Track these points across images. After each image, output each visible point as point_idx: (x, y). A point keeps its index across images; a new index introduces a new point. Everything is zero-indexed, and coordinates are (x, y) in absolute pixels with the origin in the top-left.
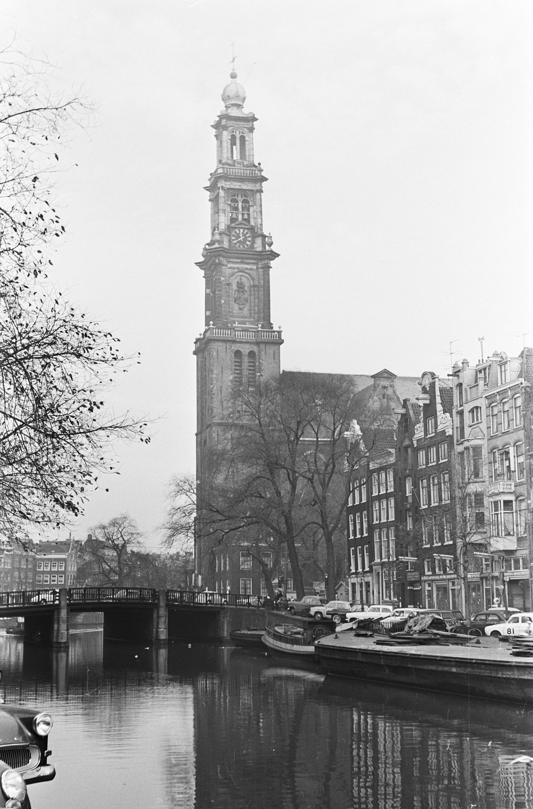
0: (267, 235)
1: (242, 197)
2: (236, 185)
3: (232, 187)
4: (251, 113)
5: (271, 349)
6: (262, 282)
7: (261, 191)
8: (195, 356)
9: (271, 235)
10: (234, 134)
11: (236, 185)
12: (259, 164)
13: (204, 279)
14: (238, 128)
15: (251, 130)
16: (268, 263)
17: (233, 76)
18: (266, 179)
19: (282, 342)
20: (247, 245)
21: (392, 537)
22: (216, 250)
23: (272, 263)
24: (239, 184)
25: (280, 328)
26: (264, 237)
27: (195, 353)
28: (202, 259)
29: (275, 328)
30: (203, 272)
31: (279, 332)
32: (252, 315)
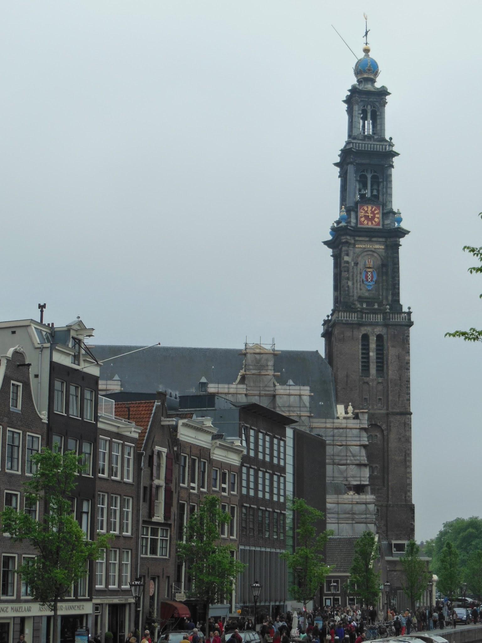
8: (323, 339)
9: (401, 211)
12: (391, 139)
13: (332, 258)
17: (367, 51)
18: (397, 154)
20: (375, 222)
21: (236, 464)
22: (345, 228)
23: (402, 241)
25: (409, 308)
26: (394, 213)
28: (330, 238)
29: (405, 309)
30: (330, 251)
31: (409, 313)
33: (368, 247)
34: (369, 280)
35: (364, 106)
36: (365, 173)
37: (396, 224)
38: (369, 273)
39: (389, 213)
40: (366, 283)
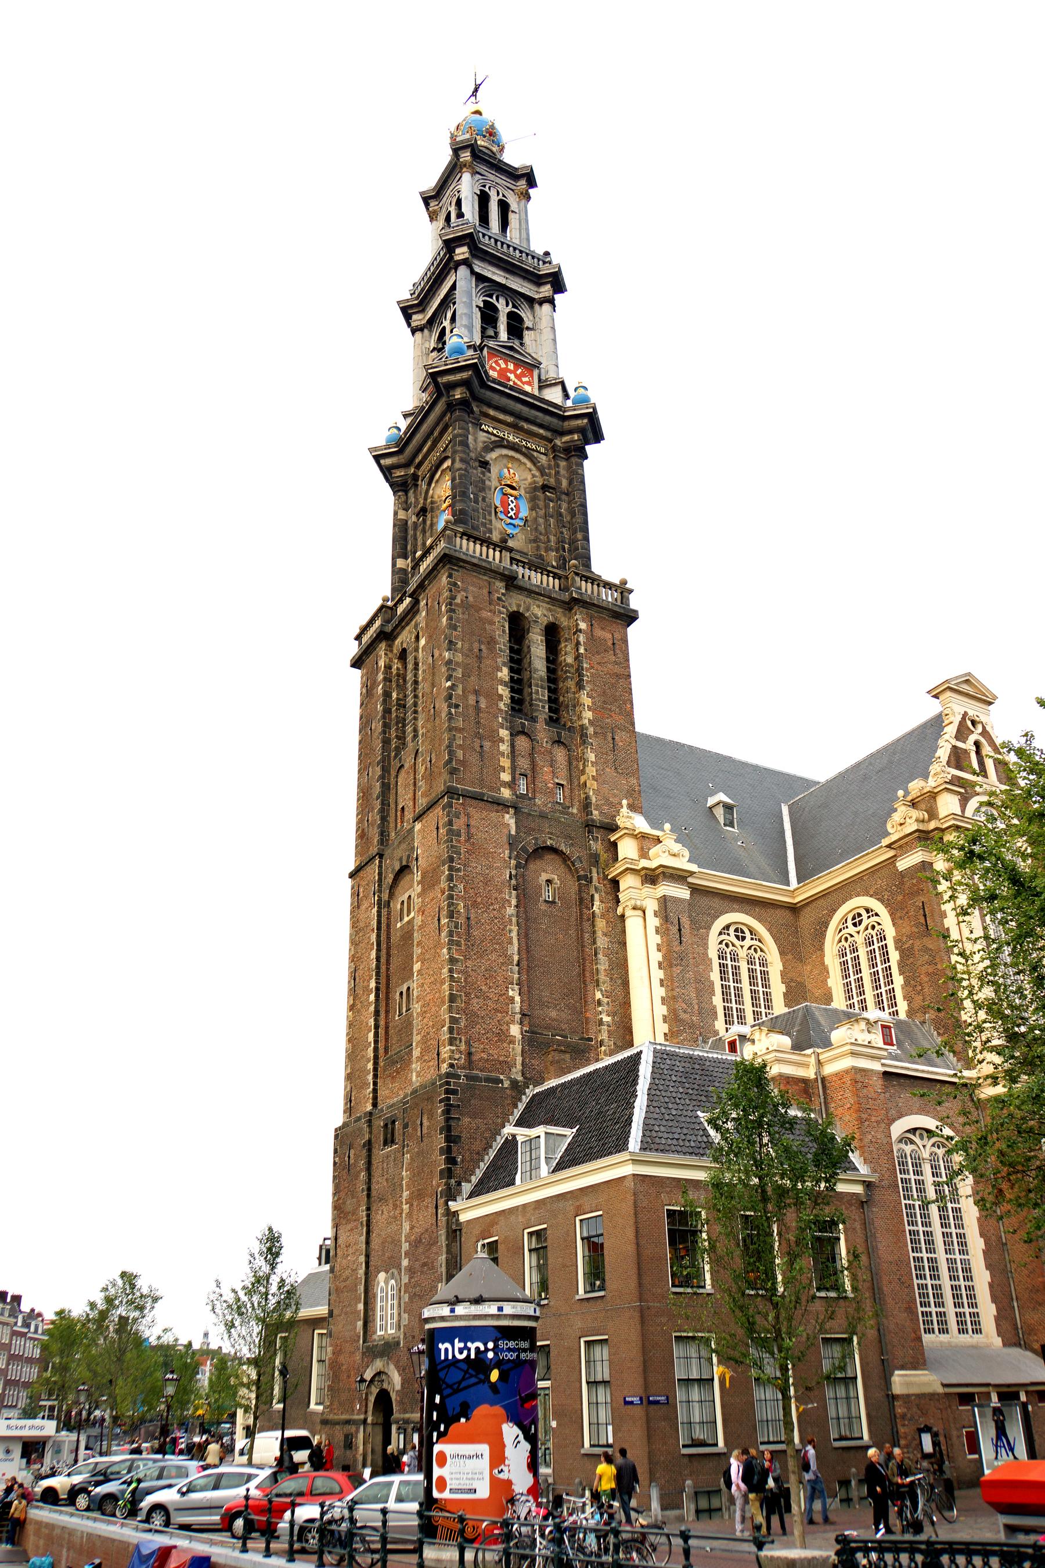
1: (507, 305)
6: (565, 483)
7: (551, 301)
8: (357, 673)
10: (487, 189)
19: (630, 617)
23: (587, 448)
27: (357, 663)
33: (511, 438)
34: (512, 513)
35: (484, 186)
36: (493, 300)
38: (512, 498)
40: (502, 516)
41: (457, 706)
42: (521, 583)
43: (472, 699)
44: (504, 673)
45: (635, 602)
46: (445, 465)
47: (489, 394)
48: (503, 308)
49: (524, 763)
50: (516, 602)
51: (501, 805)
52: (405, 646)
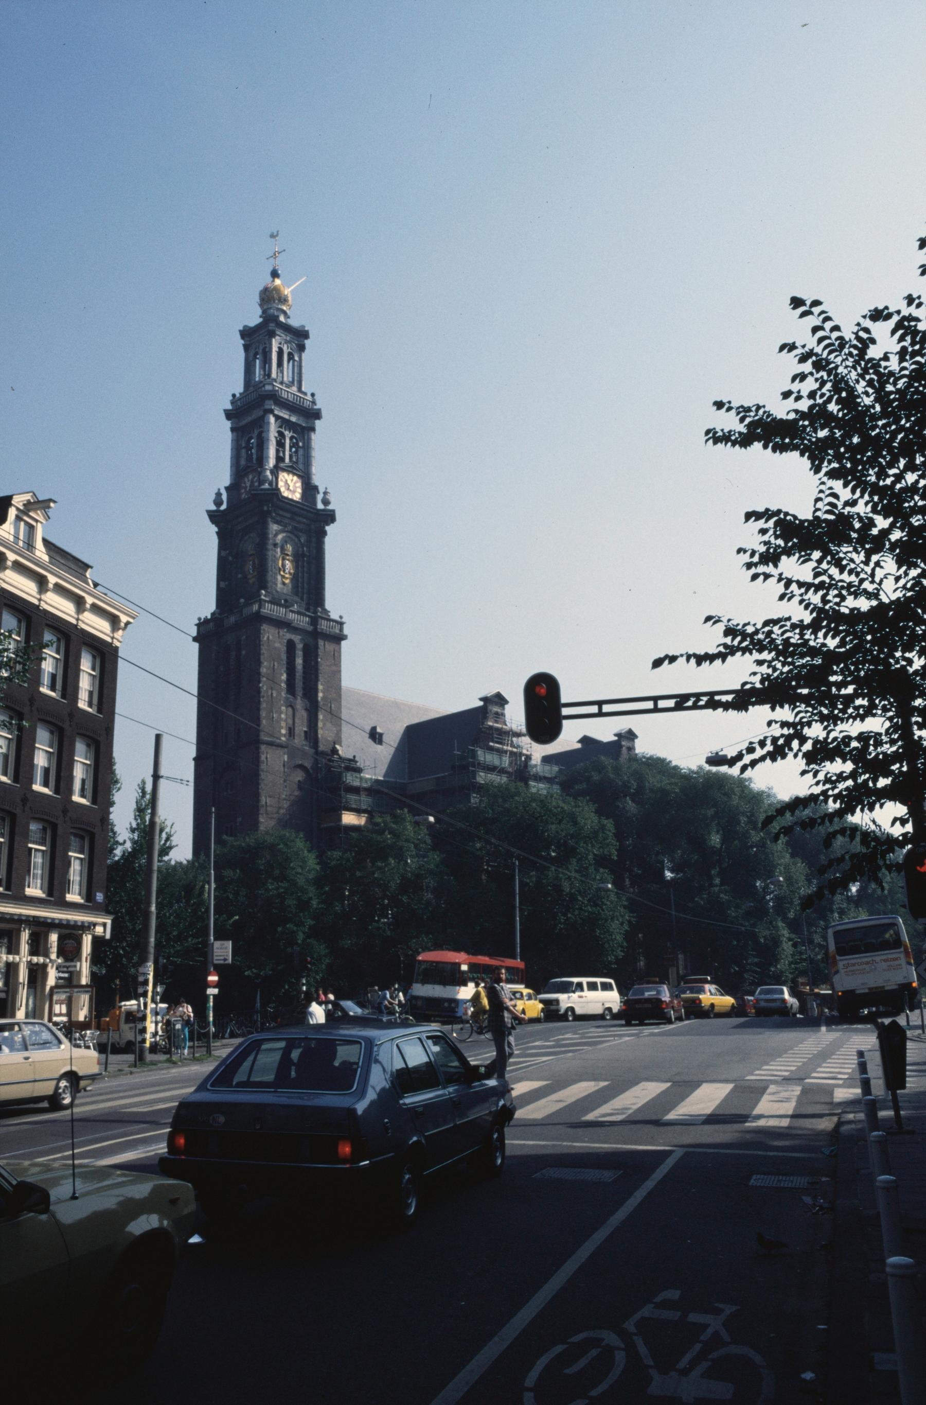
0: (322, 490)
2: (285, 415)
3: (281, 414)
4: (303, 326)
5: (330, 647)
7: (313, 429)
9: (328, 490)
10: (282, 346)
11: (285, 415)
12: (313, 395)
14: (287, 342)
15: (301, 348)
16: (324, 527)
23: (327, 528)
24: (288, 413)
31: (341, 624)
32: (300, 595)
36: (283, 430)
37: (320, 506)
39: (309, 489)
41: (263, 697)
42: (293, 625)
43: (270, 694)
44: (284, 677)
45: (346, 631)
46: (252, 535)
47: (281, 503)
48: (288, 434)
49: (290, 722)
50: (289, 636)
51: (280, 746)
52: (229, 643)
